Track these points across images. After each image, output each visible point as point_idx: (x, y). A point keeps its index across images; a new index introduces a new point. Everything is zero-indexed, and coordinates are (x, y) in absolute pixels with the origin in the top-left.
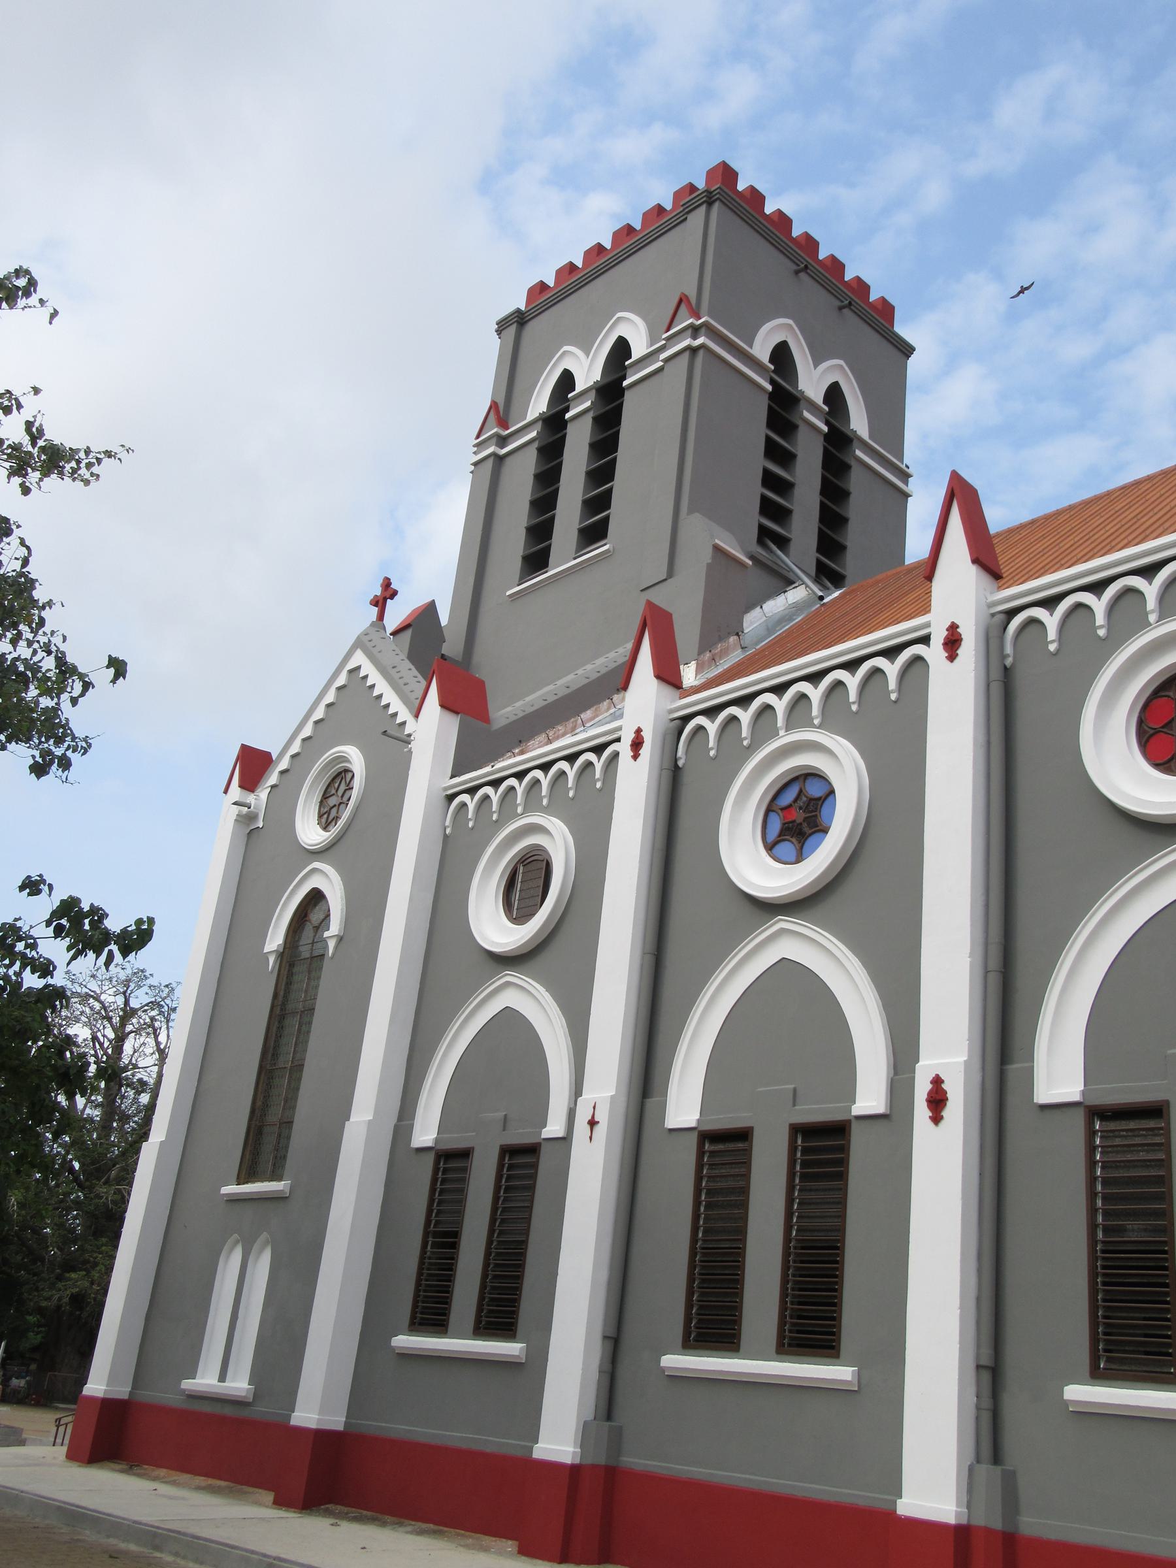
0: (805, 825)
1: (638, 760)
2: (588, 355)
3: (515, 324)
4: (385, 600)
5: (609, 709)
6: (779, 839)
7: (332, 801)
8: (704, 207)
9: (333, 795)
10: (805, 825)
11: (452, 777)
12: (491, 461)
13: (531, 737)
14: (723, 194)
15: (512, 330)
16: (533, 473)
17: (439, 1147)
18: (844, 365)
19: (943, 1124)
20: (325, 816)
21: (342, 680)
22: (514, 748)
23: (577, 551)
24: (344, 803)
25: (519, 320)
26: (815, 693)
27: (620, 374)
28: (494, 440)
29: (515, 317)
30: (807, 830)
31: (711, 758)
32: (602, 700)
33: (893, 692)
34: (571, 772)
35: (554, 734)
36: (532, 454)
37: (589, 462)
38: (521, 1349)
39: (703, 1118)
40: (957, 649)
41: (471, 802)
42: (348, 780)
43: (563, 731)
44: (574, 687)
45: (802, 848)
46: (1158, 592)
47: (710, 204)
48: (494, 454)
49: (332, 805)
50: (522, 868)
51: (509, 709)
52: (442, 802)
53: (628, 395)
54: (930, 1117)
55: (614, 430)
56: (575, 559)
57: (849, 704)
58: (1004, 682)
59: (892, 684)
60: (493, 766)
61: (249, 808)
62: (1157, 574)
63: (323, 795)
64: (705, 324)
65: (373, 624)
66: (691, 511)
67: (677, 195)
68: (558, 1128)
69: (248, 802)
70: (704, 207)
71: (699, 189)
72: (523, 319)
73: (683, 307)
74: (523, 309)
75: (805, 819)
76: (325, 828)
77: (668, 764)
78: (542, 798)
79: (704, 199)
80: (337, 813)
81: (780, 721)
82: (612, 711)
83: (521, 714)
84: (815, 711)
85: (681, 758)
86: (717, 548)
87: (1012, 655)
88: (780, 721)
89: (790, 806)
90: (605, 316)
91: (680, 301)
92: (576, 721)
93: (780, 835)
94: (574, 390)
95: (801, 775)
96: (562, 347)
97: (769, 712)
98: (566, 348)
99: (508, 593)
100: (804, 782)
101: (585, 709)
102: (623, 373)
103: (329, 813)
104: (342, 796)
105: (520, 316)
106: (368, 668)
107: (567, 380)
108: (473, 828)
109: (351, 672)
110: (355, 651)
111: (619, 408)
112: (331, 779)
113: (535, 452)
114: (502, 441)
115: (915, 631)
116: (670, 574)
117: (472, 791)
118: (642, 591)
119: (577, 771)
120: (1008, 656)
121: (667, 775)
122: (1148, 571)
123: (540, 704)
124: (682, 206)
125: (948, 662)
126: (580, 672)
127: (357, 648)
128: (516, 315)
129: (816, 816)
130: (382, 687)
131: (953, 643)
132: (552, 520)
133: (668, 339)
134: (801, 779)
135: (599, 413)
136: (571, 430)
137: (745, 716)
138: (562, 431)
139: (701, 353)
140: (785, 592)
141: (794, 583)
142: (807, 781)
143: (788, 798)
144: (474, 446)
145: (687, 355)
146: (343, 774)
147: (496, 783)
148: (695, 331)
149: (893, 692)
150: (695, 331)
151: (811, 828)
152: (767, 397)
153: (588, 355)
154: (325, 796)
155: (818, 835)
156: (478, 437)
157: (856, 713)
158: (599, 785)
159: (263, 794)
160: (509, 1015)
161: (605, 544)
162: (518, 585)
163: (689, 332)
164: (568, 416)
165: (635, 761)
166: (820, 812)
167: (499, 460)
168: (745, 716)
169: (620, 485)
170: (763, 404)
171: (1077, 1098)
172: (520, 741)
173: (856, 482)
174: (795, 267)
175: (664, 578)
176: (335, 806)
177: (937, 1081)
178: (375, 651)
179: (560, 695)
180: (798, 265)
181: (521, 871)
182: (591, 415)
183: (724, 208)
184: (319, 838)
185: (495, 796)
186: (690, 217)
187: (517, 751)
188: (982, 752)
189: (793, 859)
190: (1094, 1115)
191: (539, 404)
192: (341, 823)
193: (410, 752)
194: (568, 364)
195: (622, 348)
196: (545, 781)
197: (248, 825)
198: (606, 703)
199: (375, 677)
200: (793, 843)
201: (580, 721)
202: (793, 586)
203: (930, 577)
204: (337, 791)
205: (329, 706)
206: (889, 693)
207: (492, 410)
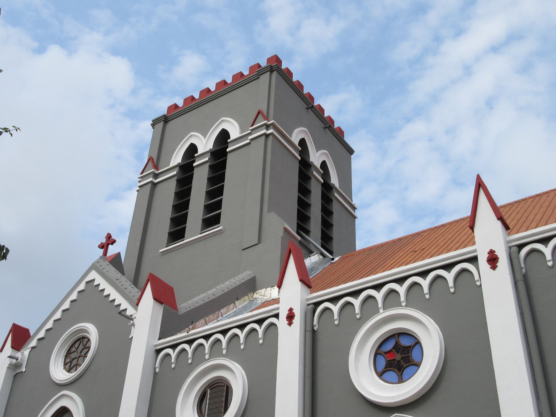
0: (402, 361)
1: (291, 326)
2: (205, 138)
3: (163, 122)
4: (108, 245)
5: (233, 308)
6: (386, 370)
7: (73, 355)
8: (269, 73)
9: (75, 351)
10: (402, 361)
11: (159, 339)
12: (150, 185)
13: (198, 320)
14: (278, 67)
15: (160, 125)
16: (174, 192)
18: (328, 153)
20: (69, 364)
21: (82, 287)
22: (189, 325)
23: (201, 231)
24: (82, 356)
25: (271, 70)
26: (402, 289)
27: (225, 146)
28: (152, 175)
29: (163, 118)
30: (405, 365)
31: (260, 344)
32: (229, 304)
33: (451, 288)
34: (242, 335)
35: (209, 319)
36: (174, 182)
37: (207, 188)
40: (496, 263)
41: (173, 354)
42: (85, 343)
43: (213, 318)
44: (218, 295)
45: (402, 374)
46: (551, 252)
47: (272, 71)
48: (151, 182)
49: (73, 357)
50: (209, 391)
51: (185, 304)
52: (153, 354)
53: (229, 156)
55: (222, 172)
56: (201, 234)
57: (424, 295)
58: (525, 281)
59: (357, 310)
60: (188, 333)
61: (17, 360)
62: (550, 242)
63: (67, 352)
64: (272, 124)
65: (101, 258)
66: (269, 211)
67: (252, 69)
69: (16, 356)
70: (269, 73)
71: (261, 67)
72: (166, 120)
73: (260, 116)
74: (166, 114)
75: (402, 358)
76: (69, 371)
77: (309, 328)
78: (222, 350)
79: (269, 69)
80: (77, 362)
81: (380, 305)
82: (235, 309)
83: (193, 307)
84: (403, 298)
85: (315, 325)
86: (285, 229)
87: (524, 268)
88: (380, 305)
89: (391, 351)
90: (215, 119)
91: (259, 113)
92: (219, 313)
93: (386, 367)
94: (169, 166)
95: (396, 334)
96: (191, 133)
97: (236, 338)
98: (192, 133)
99: (161, 251)
100: (398, 338)
101: (223, 308)
102: (226, 145)
103: (71, 362)
104: (81, 352)
105: (166, 118)
106: (99, 280)
107: (193, 149)
108: (174, 368)
109: (87, 283)
110: (91, 271)
111: (191, 177)
112: (73, 343)
113: (176, 182)
114: (156, 176)
115: (462, 256)
116: (259, 241)
117: (174, 347)
118: (243, 250)
119: (176, 354)
120: (523, 268)
121: (309, 334)
122: (545, 241)
123: (201, 303)
124: (257, 72)
125: (492, 270)
126: (218, 287)
127: (93, 269)
128: (164, 117)
129: (409, 356)
130: (109, 290)
131: (493, 260)
132: (186, 215)
133: (252, 130)
134: (396, 336)
135: (212, 164)
136: (196, 172)
137: (356, 302)
138: (191, 172)
139: (271, 137)
140: (310, 256)
141: (313, 252)
142: (399, 337)
143: (389, 346)
144: (139, 178)
145: (264, 137)
146: (82, 339)
147: (190, 342)
148: (267, 127)
149: (451, 288)
150: (267, 127)
151: (406, 364)
152: (298, 162)
153: (205, 138)
154: (69, 353)
155: (413, 368)
156: (142, 173)
157: (429, 299)
158: (261, 341)
159: (26, 352)
161: (219, 227)
162: (166, 247)
163: (265, 127)
164: (194, 164)
165: (290, 326)
166: (411, 354)
167: (154, 185)
169: (226, 198)
170: (297, 166)
172: (192, 322)
173: (335, 207)
174: (306, 106)
175: (257, 243)
176: (76, 358)
178: (104, 271)
179: (211, 299)
180: (308, 106)
181: (209, 392)
182: (208, 164)
183: (278, 75)
184: (63, 376)
186: (261, 77)
187: (191, 327)
188: (519, 317)
189: (397, 381)
191: (177, 158)
192: (80, 369)
193: (133, 325)
194: (194, 141)
195: (224, 135)
196: (224, 341)
197: (15, 370)
198: (232, 305)
199: (104, 284)
200: (395, 372)
201: (220, 314)
202: (313, 254)
203: (472, 227)
204: (77, 350)
205: (72, 301)
206: (356, 315)
207: (150, 161)
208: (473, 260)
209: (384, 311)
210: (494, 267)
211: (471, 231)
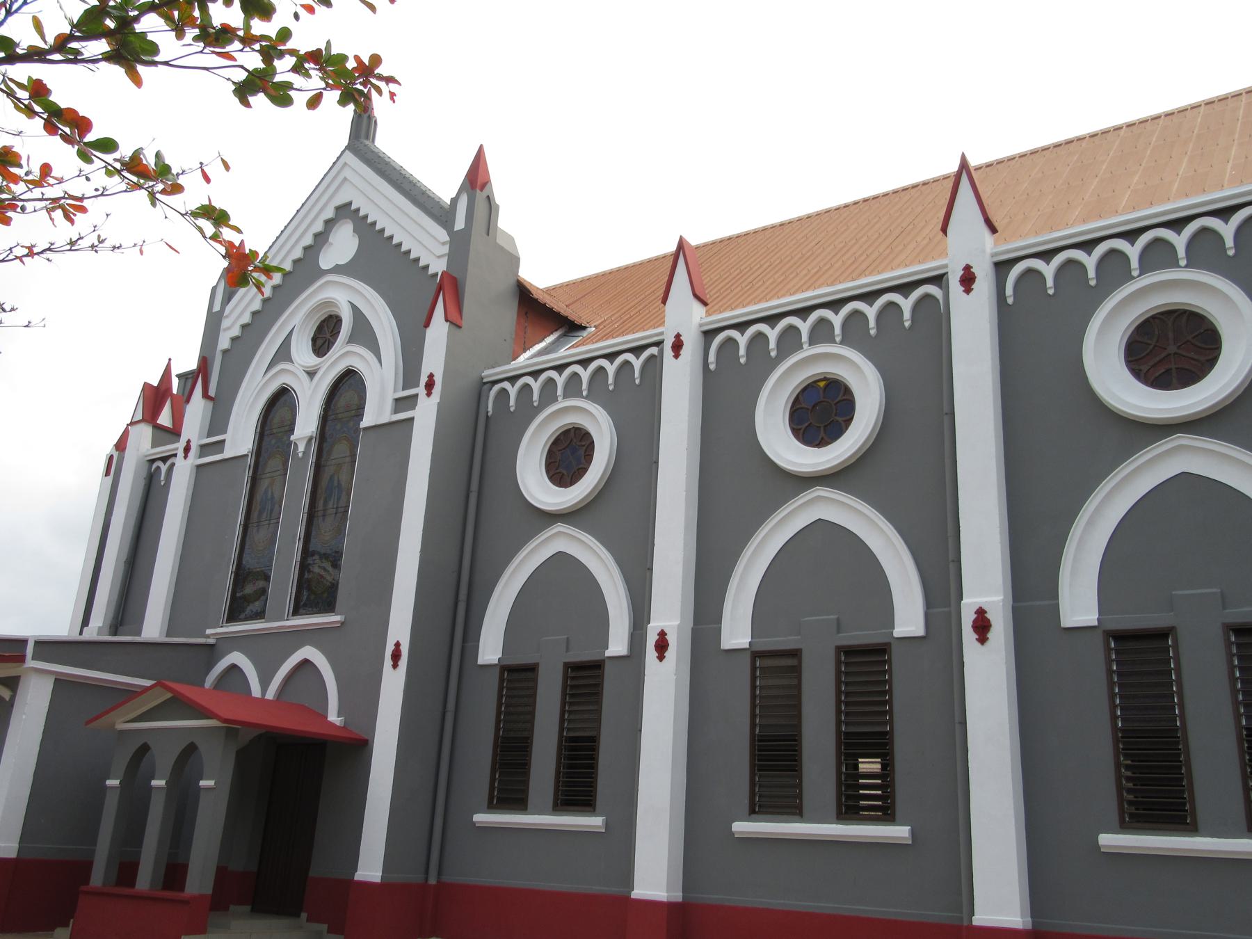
17: (502, 664)
19: (988, 643)
38: (603, 820)
39: (754, 640)
54: (976, 639)
68: (620, 649)
84: (838, 330)
88: (805, 338)
125: (965, 294)
137: (772, 334)
160: (561, 560)
168: (772, 334)
171: (1096, 623)
177: (981, 612)
185: (536, 386)
190: (1110, 636)
208: (939, 280)
209: (810, 345)
210: (968, 290)
211: (941, 233)
